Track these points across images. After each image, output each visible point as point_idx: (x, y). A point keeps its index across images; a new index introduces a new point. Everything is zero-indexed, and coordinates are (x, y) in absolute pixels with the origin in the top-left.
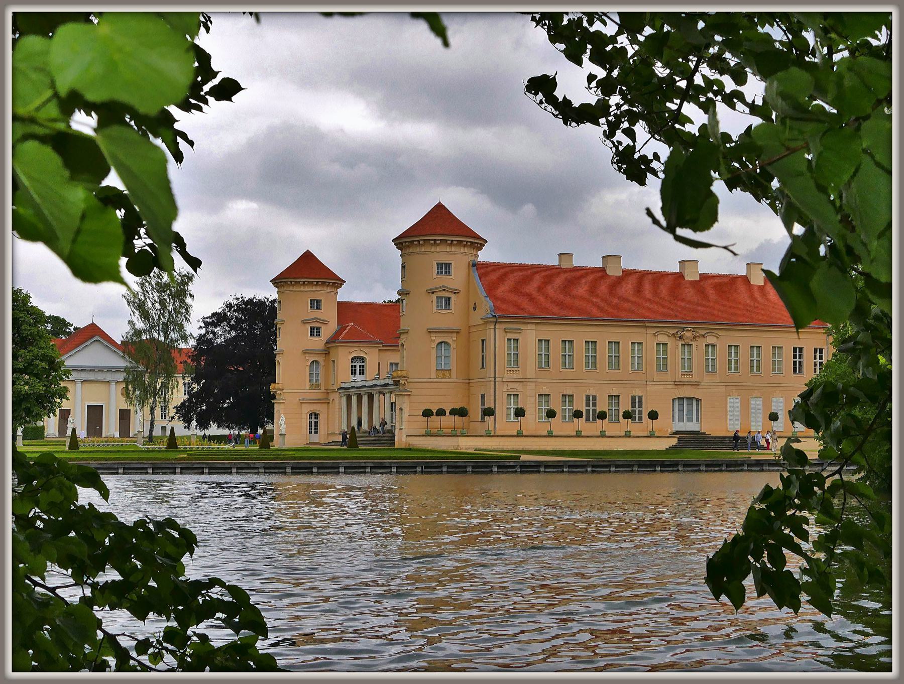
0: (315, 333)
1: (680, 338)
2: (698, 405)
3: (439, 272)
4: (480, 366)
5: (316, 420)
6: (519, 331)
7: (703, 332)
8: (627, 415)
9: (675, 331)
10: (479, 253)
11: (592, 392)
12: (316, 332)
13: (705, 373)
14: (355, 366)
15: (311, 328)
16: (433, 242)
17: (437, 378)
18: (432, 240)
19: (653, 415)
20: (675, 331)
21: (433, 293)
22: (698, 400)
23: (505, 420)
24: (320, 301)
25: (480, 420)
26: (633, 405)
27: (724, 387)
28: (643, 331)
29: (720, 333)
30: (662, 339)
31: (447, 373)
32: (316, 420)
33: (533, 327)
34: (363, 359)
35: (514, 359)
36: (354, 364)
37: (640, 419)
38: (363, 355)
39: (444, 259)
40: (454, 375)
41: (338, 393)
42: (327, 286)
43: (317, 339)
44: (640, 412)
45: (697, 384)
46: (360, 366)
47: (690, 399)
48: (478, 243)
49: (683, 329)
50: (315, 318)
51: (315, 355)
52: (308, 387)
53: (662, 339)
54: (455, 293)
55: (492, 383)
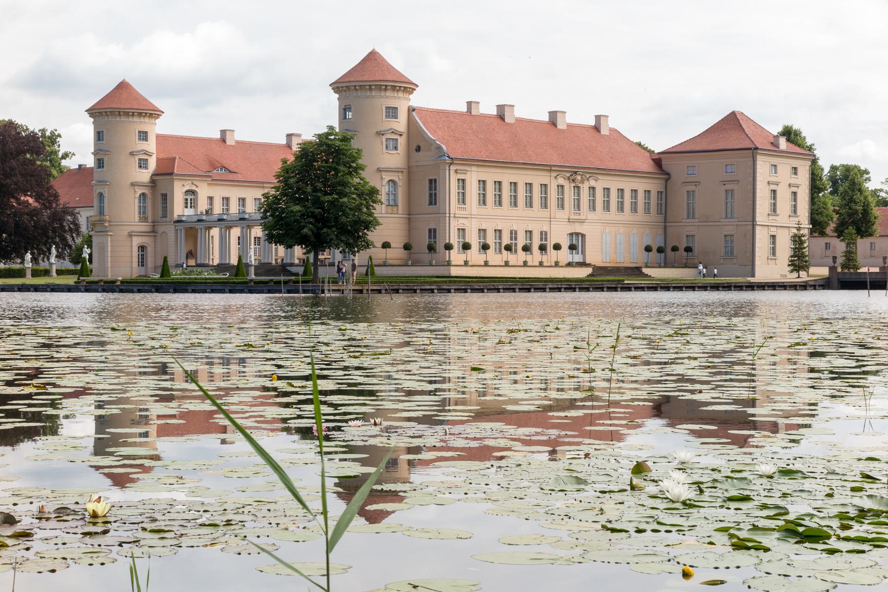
1: (573, 181)
2: (582, 237)
3: (387, 116)
4: (427, 203)
5: (143, 253)
6: (465, 172)
7: (588, 176)
8: (508, 248)
9: (568, 175)
10: (411, 96)
11: (515, 228)
12: (143, 164)
13: (572, 212)
15: (140, 160)
16: (368, 87)
17: (387, 213)
18: (383, 85)
19: (557, 247)
20: (568, 175)
21: (383, 134)
22: (583, 236)
24: (146, 133)
26: (511, 239)
27: (600, 224)
28: (548, 174)
29: (600, 177)
30: (561, 181)
31: (395, 209)
32: (143, 253)
33: (474, 168)
34: (193, 193)
35: (463, 199)
36: (186, 197)
37: (516, 251)
38: (194, 188)
39: (392, 103)
40: (400, 212)
41: (173, 226)
42: (144, 116)
43: (146, 171)
44: (516, 244)
45: (582, 222)
46: (191, 200)
47: (577, 234)
48: (410, 88)
49: (576, 173)
50: (143, 150)
51: (142, 188)
52: (137, 219)
53: (561, 181)
54: (401, 135)
55: (447, 218)
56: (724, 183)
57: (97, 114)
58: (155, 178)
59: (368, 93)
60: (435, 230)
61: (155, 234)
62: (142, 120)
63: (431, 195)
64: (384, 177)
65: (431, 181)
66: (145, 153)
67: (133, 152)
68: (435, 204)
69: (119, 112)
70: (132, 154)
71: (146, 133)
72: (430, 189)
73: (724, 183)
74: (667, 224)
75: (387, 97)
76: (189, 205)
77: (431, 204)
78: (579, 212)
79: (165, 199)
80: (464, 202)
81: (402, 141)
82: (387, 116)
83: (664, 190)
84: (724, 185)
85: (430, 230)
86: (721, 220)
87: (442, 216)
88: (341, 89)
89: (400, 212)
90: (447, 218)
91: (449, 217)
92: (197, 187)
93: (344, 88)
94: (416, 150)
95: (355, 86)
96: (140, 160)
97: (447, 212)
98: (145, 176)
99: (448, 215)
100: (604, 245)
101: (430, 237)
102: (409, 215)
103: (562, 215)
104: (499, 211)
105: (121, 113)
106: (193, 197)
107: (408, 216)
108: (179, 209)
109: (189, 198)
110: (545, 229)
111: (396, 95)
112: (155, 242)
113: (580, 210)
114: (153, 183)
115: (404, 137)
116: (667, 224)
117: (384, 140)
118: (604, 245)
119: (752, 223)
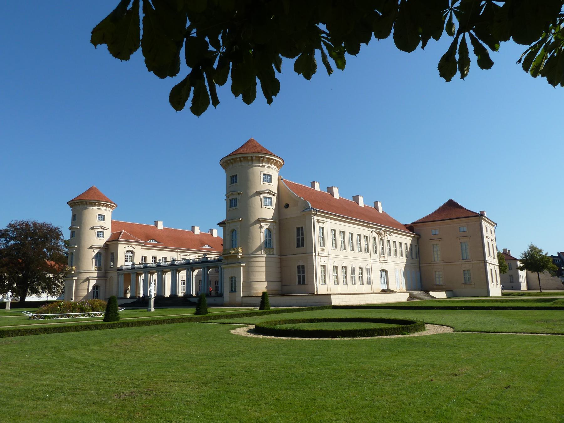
0: (100, 235)
1: (381, 235)
4: (296, 245)
5: (97, 291)
12: (101, 234)
14: (127, 256)
21: (261, 194)
23: (321, 283)
24: (104, 216)
25: (297, 283)
32: (97, 291)
36: (126, 255)
38: (132, 249)
40: (275, 253)
41: (117, 273)
46: (130, 256)
56: (459, 238)
57: (73, 204)
58: (108, 243)
59: (250, 163)
60: (303, 267)
61: (106, 278)
62: (101, 207)
63: (298, 240)
64: (263, 225)
65: (298, 229)
66: (101, 228)
67: (93, 227)
68: (303, 246)
69: (86, 202)
70: (92, 228)
71: (104, 216)
72: (298, 235)
73: (459, 238)
74: (421, 265)
75: (264, 166)
76: (129, 260)
77: (298, 246)
78: (384, 256)
79: (114, 256)
80: (324, 245)
81: (274, 199)
82: (264, 181)
83: (417, 245)
84: (460, 239)
85: (299, 267)
86: (460, 261)
87: (309, 254)
88: (229, 162)
89: (275, 253)
90: (314, 256)
91: (315, 255)
92: (134, 249)
93: (231, 161)
94: (285, 207)
95: (240, 158)
96: (98, 232)
97: (314, 252)
98: (101, 242)
99: (314, 254)
100: (396, 277)
101: (299, 272)
102: (281, 256)
103: (376, 257)
104: (343, 252)
105: (87, 203)
106: (132, 255)
107: (279, 257)
108: (122, 262)
109: (129, 255)
110: (369, 267)
111: (270, 166)
112: (106, 283)
113: (384, 255)
114: (107, 246)
115: (276, 197)
116: (421, 265)
117: (262, 198)
118: (396, 277)
119: (483, 261)
